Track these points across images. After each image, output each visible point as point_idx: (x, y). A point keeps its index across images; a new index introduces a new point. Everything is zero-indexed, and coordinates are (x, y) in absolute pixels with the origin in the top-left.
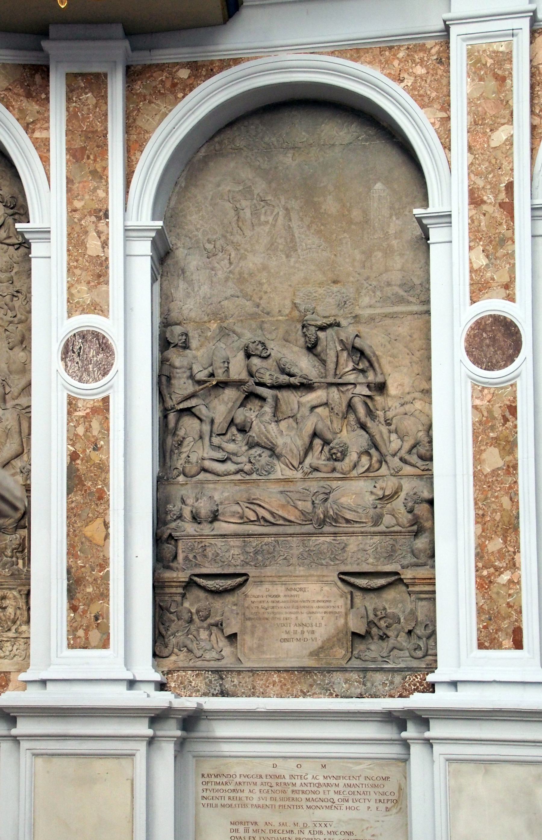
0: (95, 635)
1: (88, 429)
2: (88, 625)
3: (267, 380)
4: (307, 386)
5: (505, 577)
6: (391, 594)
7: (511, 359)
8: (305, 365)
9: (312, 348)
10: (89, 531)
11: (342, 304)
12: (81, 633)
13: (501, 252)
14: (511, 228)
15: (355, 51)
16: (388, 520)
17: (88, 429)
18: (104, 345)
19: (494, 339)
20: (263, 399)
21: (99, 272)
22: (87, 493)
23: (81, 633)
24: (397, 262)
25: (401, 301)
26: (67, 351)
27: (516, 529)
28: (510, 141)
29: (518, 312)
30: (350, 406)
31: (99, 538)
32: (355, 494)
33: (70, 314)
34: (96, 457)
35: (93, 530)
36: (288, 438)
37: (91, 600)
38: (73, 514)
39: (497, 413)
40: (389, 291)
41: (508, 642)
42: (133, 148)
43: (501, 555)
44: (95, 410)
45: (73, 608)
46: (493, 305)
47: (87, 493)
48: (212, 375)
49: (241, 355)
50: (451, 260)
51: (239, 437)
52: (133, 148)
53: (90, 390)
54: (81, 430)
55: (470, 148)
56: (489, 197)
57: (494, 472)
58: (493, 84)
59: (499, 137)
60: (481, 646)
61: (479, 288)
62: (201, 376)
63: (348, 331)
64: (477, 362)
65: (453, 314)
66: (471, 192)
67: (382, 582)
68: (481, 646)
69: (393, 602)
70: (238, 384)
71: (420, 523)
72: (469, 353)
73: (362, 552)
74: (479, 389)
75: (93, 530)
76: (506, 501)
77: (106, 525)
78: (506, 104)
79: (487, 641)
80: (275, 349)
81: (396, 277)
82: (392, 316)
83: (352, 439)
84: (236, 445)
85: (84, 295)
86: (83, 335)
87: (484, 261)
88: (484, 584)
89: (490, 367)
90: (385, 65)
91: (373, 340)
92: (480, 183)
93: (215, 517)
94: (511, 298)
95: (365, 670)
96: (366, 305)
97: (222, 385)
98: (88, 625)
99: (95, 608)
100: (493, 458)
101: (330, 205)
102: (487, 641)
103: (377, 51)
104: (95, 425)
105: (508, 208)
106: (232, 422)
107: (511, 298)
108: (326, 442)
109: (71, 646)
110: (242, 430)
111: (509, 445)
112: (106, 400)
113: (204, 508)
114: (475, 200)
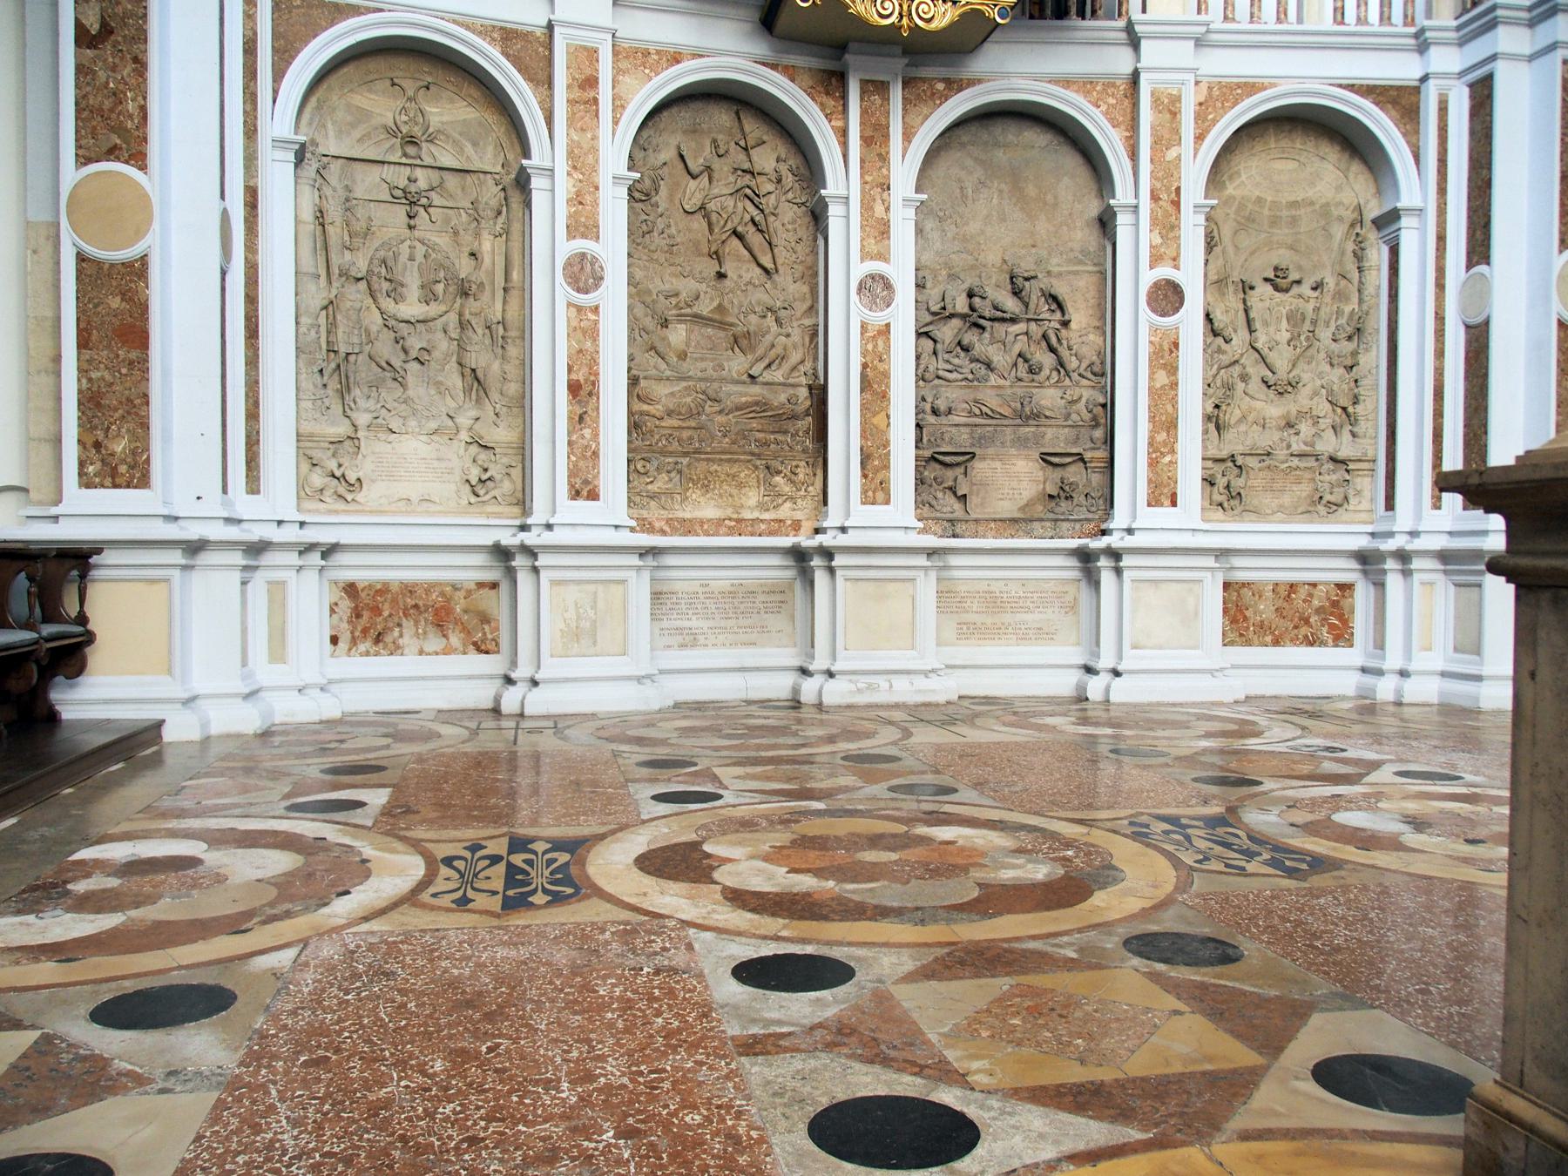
0: (880, 496)
1: (875, 346)
2: (876, 488)
3: (987, 314)
4: (1013, 320)
5: (1167, 459)
6: (1072, 469)
7: (1176, 310)
8: (1011, 305)
9: (1017, 293)
10: (875, 421)
11: (1038, 262)
12: (870, 493)
13: (1171, 235)
14: (1178, 219)
16: (1074, 417)
17: (875, 346)
18: (888, 285)
19: (1166, 296)
20: (984, 329)
21: (883, 230)
22: (874, 393)
23: (870, 493)
24: (1079, 235)
25: (1081, 262)
26: (861, 287)
27: (1176, 427)
28: (1179, 158)
30: (1045, 337)
31: (883, 426)
33: (862, 260)
34: (881, 367)
35: (879, 420)
36: (1000, 359)
37: (877, 470)
38: (864, 408)
39: (1166, 347)
40: (1071, 255)
41: (1167, 502)
42: (908, 137)
43: (1165, 444)
44: (880, 332)
45: (865, 476)
46: (1165, 272)
47: (874, 393)
48: (944, 308)
49: (964, 295)
51: (962, 354)
52: (908, 137)
53: (878, 318)
54: (870, 347)
55: (1152, 160)
56: (1164, 196)
57: (1162, 387)
58: (1168, 116)
59: (1171, 154)
60: (1149, 505)
61: (1155, 260)
62: (935, 308)
63: (1043, 282)
64: (1154, 311)
66: (1152, 191)
67: (1069, 460)
68: (1149, 505)
70: (964, 317)
72: (1149, 304)
74: (1154, 330)
75: (879, 420)
76: (1169, 408)
77: (888, 417)
78: (1176, 131)
79: (1153, 502)
80: (990, 292)
81: (1077, 246)
82: (1076, 273)
84: (962, 360)
85: (873, 247)
86: (872, 277)
87: (1159, 241)
88: (1153, 463)
89: (1163, 315)
90: (1087, 94)
91: (1061, 290)
92: (1158, 185)
93: (950, 411)
94: (1177, 267)
95: (1056, 520)
96: (1055, 264)
97: (952, 316)
98: (876, 488)
99: (880, 476)
100: (1162, 378)
101: (1031, 190)
102: (1153, 502)
104: (880, 343)
105: (1177, 204)
106: (959, 343)
107: (1177, 267)
108: (1026, 361)
109: (863, 503)
110: (966, 349)
111: (1173, 370)
112: (888, 325)
113: (942, 405)
114: (1155, 197)
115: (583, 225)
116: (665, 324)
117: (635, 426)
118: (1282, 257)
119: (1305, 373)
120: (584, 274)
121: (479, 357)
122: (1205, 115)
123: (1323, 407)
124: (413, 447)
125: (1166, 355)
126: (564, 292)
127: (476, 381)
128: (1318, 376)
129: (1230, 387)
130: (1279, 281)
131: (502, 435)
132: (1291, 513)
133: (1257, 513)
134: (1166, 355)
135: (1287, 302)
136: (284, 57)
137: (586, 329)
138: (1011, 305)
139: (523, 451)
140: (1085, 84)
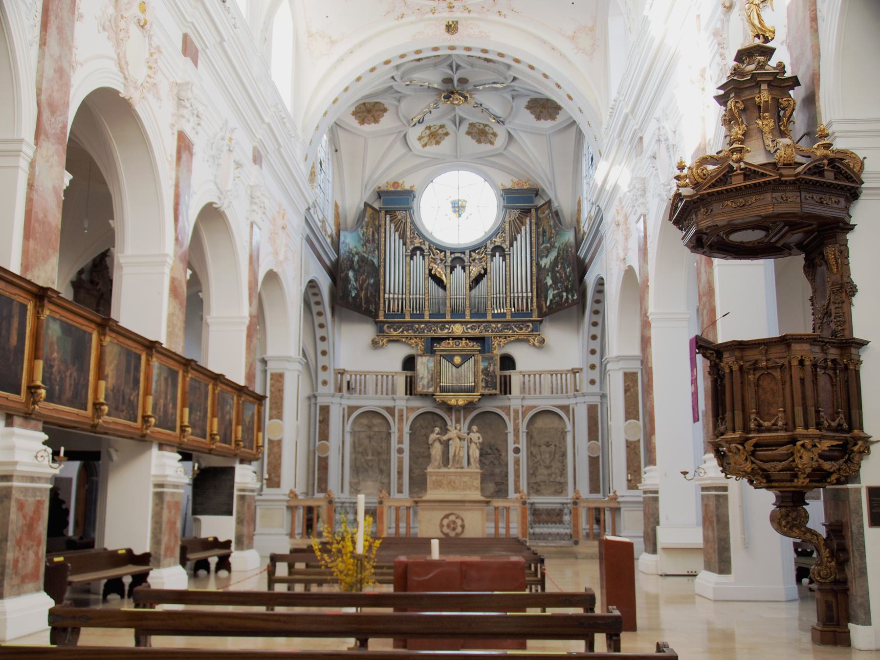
8: (490, 451)
15: (497, 407)
29: (520, 446)
32: (497, 471)
42: (465, 419)
46: (517, 445)
50: (511, 438)
52: (465, 419)
61: (515, 443)
65: (511, 446)
69: (502, 487)
71: (506, 475)
73: (498, 479)
83: (496, 462)
91: (499, 448)
103: (501, 408)
111: (518, 465)
115: (400, 441)
116: (418, 458)
117: (411, 478)
118: (547, 439)
119: (553, 464)
120: (400, 451)
121: (382, 466)
122: (524, 414)
123: (558, 471)
124: (370, 483)
125: (517, 462)
126: (397, 455)
127: (381, 471)
128: (556, 465)
129: (536, 468)
130: (548, 445)
131: (386, 481)
132: (550, 495)
133: (543, 495)
134: (517, 462)
135: (548, 449)
136: (349, 416)
137: (400, 462)
138: (490, 451)
139: (389, 484)
140: (501, 408)
